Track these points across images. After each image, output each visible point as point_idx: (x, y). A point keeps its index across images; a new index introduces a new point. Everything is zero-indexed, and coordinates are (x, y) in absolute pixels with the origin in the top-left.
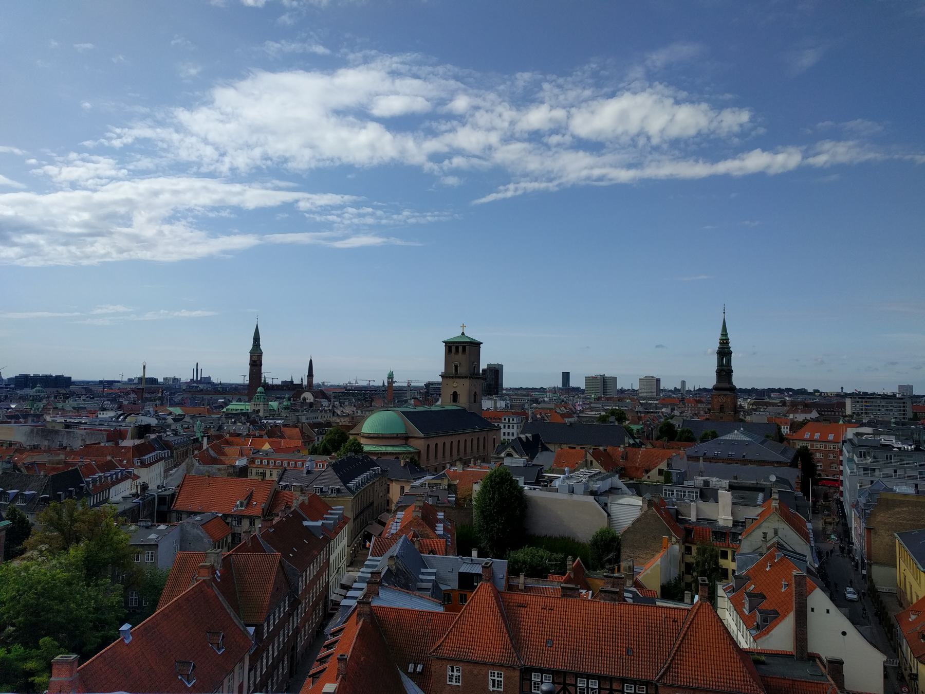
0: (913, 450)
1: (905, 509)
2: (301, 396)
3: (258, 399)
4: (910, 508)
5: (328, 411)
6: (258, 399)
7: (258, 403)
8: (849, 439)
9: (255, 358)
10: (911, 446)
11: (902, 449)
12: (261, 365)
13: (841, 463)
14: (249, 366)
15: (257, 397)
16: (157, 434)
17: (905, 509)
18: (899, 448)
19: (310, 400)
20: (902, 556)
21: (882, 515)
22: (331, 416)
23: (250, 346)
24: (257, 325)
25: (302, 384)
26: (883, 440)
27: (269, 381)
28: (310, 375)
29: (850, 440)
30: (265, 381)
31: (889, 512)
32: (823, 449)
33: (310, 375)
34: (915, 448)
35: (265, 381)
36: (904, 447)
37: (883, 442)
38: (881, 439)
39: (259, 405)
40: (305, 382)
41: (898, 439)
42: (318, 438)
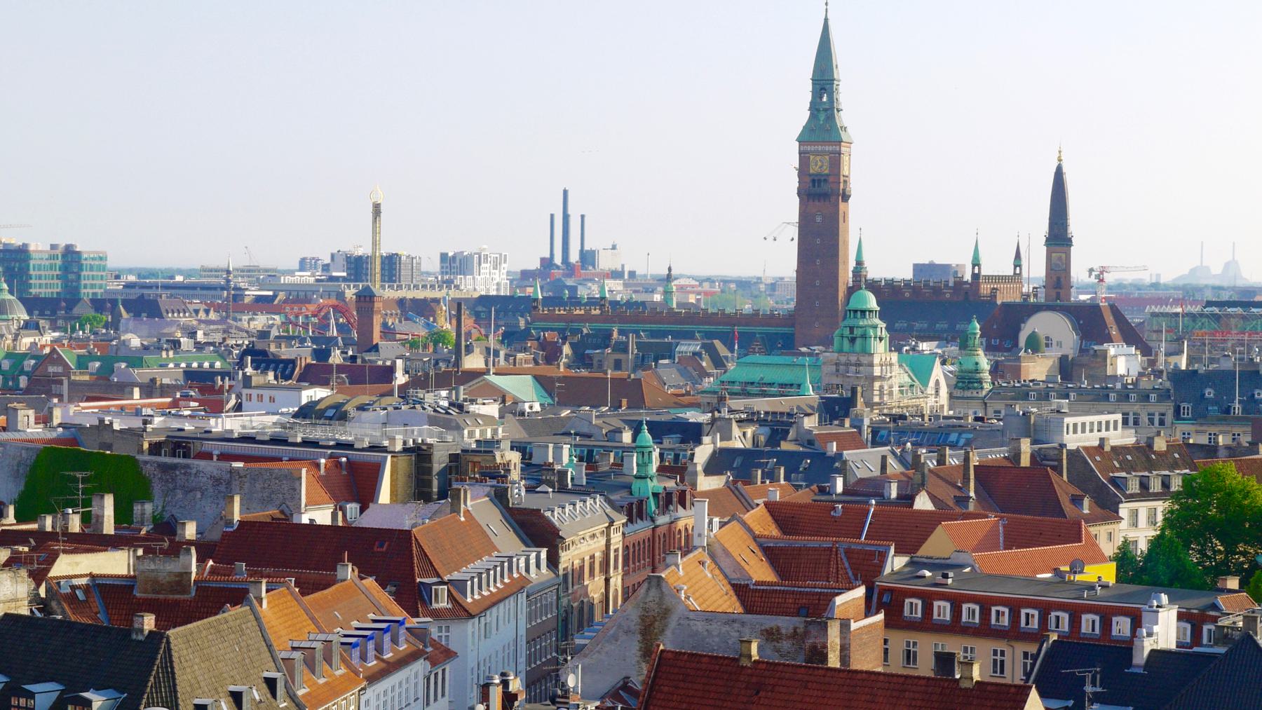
2: (1018, 330)
3: (853, 340)
5: (1153, 396)
6: (853, 340)
7: (853, 359)
9: (819, 166)
12: (846, 198)
14: (797, 199)
15: (847, 332)
16: (494, 482)
19: (1059, 344)
22: (1169, 418)
23: (802, 116)
24: (826, 20)
25: (1016, 277)
27: (875, 271)
28: (1059, 237)
30: (859, 263)
33: (1059, 237)
35: (859, 263)
39: (859, 364)
40: (1036, 269)
42: (1135, 514)
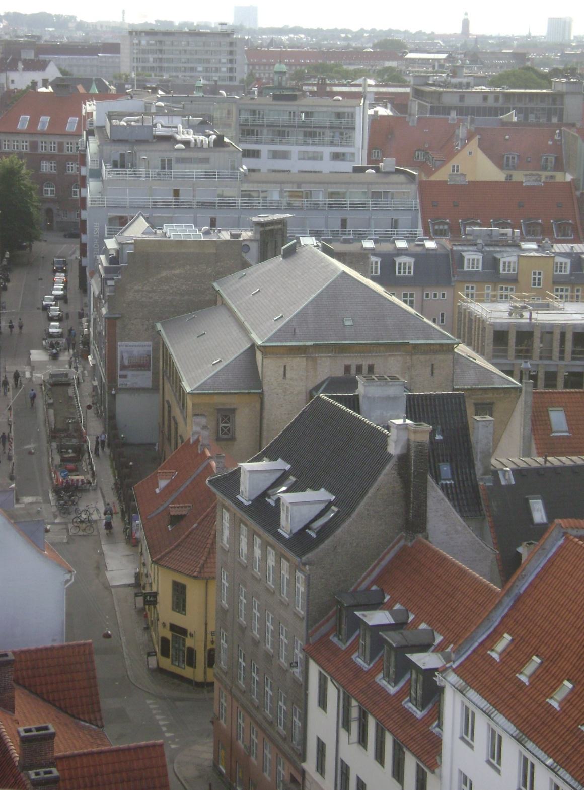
0: (212, 145)
1: (177, 272)
4: (188, 267)
8: (97, 127)
10: (208, 136)
11: (192, 145)
13: (83, 183)
17: (177, 272)
18: (187, 143)
20: (166, 368)
21: (136, 288)
26: (159, 126)
29: (102, 128)
31: (151, 280)
32: (56, 152)
34: (215, 141)
36: (196, 141)
37: (159, 131)
38: (155, 126)
41: (189, 125)
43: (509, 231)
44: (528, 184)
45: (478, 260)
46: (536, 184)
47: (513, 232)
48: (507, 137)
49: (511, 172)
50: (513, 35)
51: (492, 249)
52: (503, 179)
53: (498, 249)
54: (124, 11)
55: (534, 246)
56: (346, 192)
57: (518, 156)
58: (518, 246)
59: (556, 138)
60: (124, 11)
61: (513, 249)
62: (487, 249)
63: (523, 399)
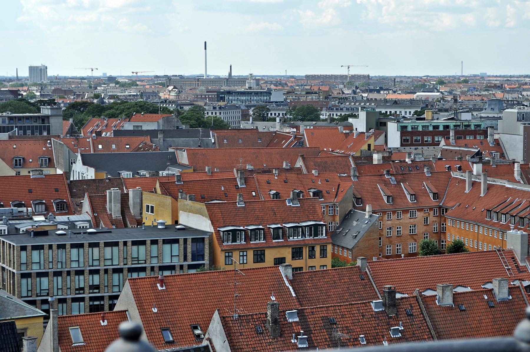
43: (24, 209)
44: (34, 177)
45: (4, 230)
46: (40, 176)
47: (27, 210)
48: (15, 146)
49: (18, 170)
50: (88, 76)
51: (14, 222)
52: (14, 175)
53: (18, 222)
54: (205, 43)
55: (42, 218)
56: (353, 157)
57: (23, 159)
58: (31, 219)
59: (48, 145)
60: (205, 43)
61: (29, 221)
62: (11, 222)
63: (52, 322)
